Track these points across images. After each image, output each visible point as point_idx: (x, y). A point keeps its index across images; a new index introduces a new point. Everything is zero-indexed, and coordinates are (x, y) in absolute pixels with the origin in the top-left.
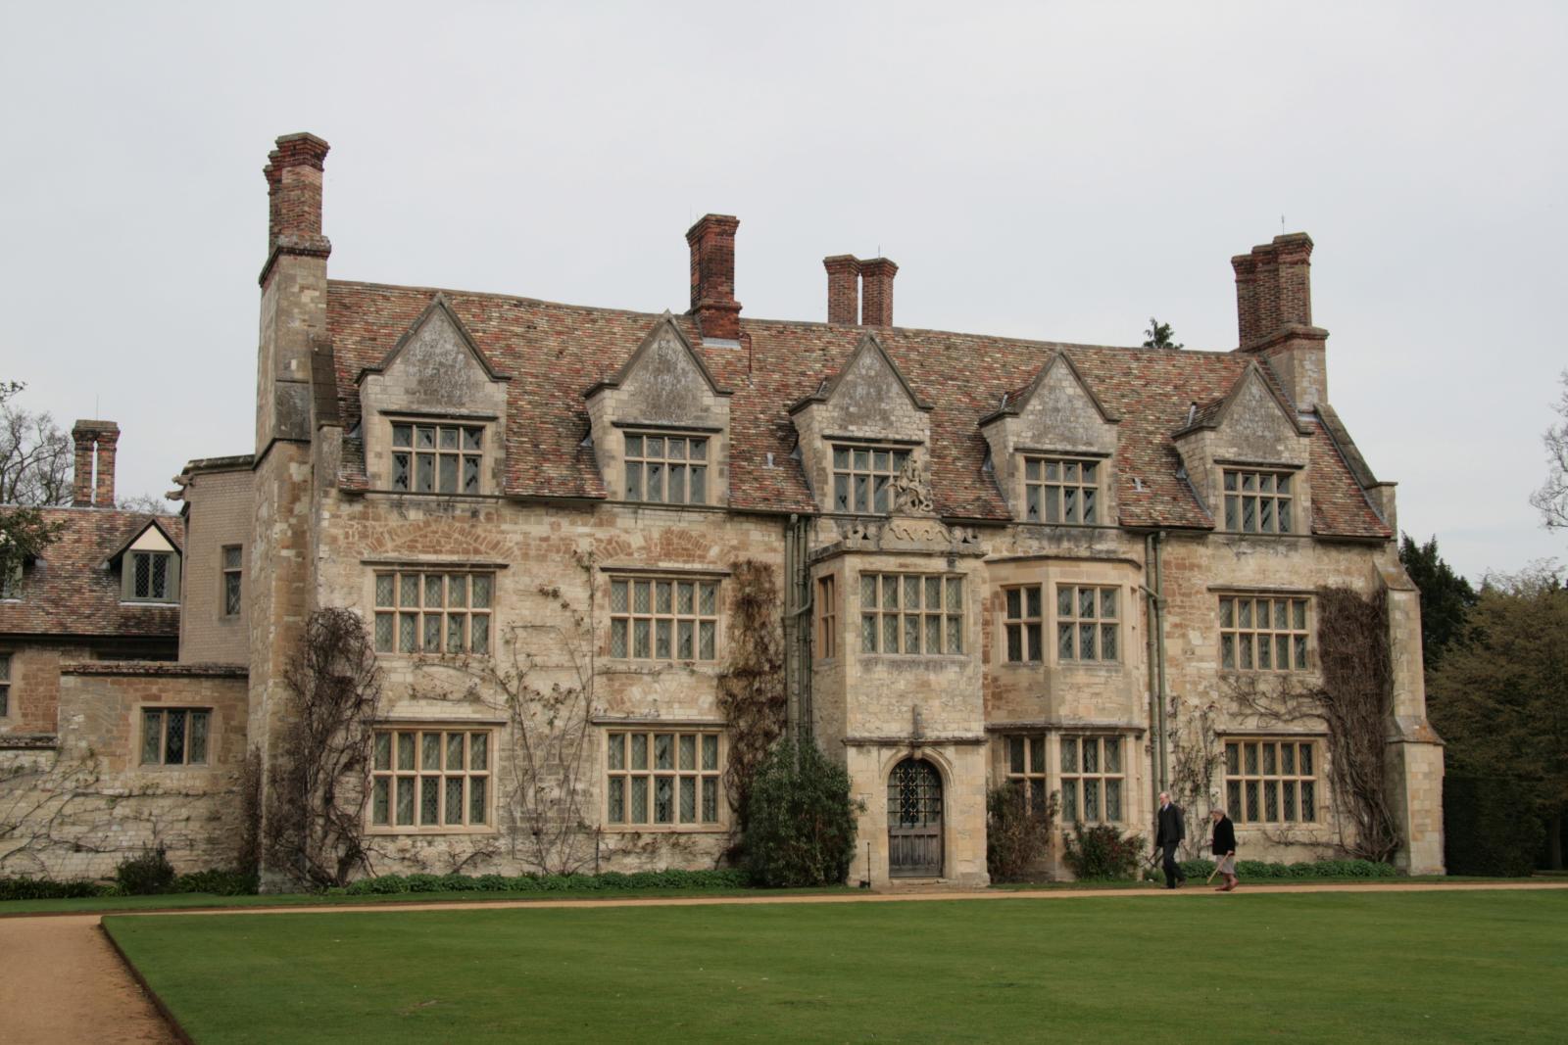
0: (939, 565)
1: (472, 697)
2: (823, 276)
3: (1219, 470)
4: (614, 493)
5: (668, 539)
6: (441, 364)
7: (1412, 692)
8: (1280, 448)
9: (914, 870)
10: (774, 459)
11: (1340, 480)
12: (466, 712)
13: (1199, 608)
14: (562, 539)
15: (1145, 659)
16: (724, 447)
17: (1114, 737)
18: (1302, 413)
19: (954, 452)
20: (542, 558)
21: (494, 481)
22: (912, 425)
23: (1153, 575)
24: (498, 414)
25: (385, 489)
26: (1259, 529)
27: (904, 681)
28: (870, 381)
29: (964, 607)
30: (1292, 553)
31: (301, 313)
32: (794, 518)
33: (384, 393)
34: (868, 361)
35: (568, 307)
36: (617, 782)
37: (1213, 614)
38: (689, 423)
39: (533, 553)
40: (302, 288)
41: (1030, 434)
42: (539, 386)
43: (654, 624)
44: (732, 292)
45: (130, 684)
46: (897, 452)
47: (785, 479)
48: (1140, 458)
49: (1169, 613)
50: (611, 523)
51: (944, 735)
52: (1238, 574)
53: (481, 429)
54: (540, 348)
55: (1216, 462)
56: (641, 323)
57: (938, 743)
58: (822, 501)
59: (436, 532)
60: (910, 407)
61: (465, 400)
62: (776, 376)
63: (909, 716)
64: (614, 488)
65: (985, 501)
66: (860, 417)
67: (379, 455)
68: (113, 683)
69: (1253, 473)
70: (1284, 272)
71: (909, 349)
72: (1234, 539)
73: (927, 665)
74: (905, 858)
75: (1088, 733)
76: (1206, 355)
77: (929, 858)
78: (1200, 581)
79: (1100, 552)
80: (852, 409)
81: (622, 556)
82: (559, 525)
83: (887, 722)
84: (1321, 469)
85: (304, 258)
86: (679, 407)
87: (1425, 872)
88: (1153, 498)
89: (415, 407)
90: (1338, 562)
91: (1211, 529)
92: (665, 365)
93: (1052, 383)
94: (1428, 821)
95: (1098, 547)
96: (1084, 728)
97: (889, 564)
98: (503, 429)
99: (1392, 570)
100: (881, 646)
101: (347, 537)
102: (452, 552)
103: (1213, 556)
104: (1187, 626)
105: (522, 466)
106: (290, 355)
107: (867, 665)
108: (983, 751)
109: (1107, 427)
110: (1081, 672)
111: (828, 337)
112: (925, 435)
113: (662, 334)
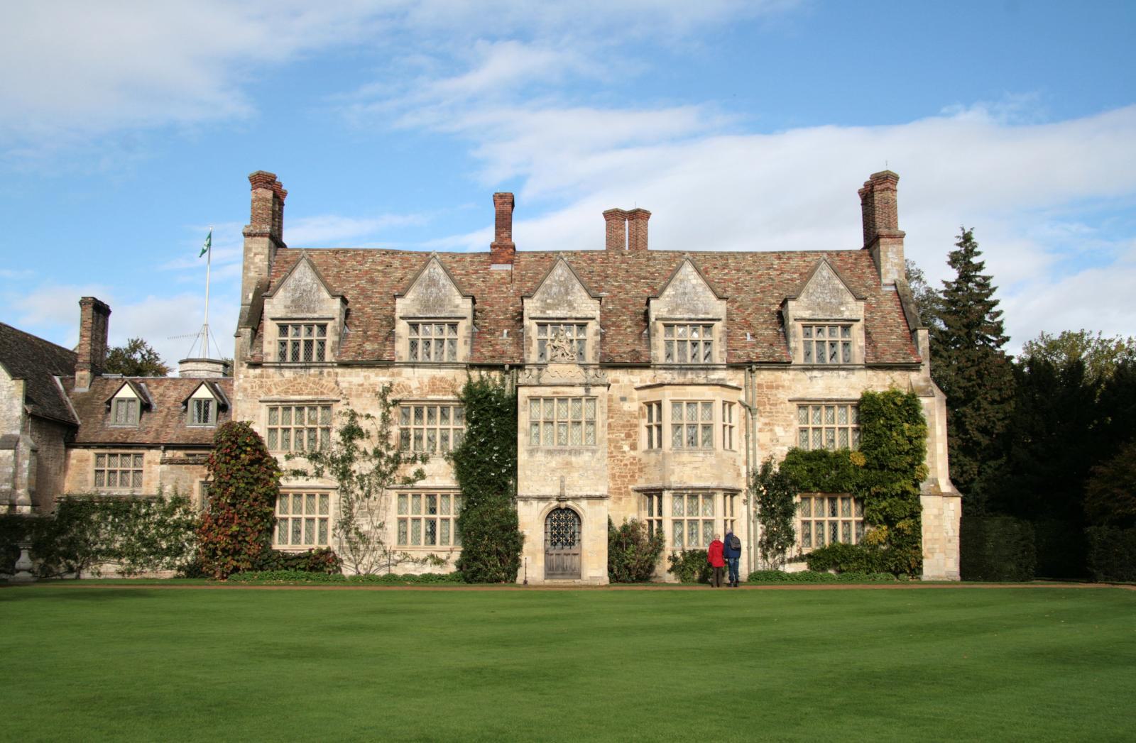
0: (580, 391)
1: (319, 474)
2: (603, 221)
3: (798, 325)
4: (401, 357)
5: (433, 382)
6: (304, 290)
7: (932, 463)
8: (843, 309)
9: (562, 574)
10: (508, 333)
12: (314, 482)
13: (783, 413)
14: (370, 385)
15: (744, 445)
16: (467, 328)
17: (709, 494)
18: (886, 285)
19: (629, 323)
20: (359, 396)
21: (332, 354)
22: (588, 308)
23: (750, 393)
24: (335, 316)
25: (272, 361)
26: (828, 361)
27: (555, 462)
28: (560, 284)
29: (597, 416)
30: (851, 376)
31: (255, 268)
32: (507, 367)
33: (275, 307)
34: (560, 272)
35: (416, 253)
36: (402, 521)
37: (792, 416)
38: (447, 315)
39: (354, 393)
40: (255, 254)
41: (666, 309)
42: (381, 299)
43: (425, 431)
44: (510, 237)
45: (193, 469)
48: (758, 319)
49: (761, 416)
50: (399, 374)
51: (580, 494)
52: (810, 390)
54: (389, 278)
55: (795, 320)
56: (457, 258)
57: (575, 499)
58: (529, 356)
59: (299, 383)
60: (587, 298)
61: (317, 309)
62: (529, 284)
63: (558, 482)
64: (400, 354)
65: (638, 352)
66: (555, 305)
68: (185, 468)
69: (824, 326)
70: (877, 196)
71: (623, 262)
72: (807, 368)
73: (570, 452)
74: (558, 567)
75: (690, 492)
76: (829, 253)
77: (573, 567)
78: (783, 395)
79: (713, 380)
80: (548, 301)
82: (369, 377)
83: (543, 486)
84: (887, 321)
85: (256, 238)
86: (440, 306)
87: (932, 579)
88: (754, 346)
89: (289, 315)
90: (884, 380)
91: (790, 363)
92: (433, 282)
93: (681, 278)
94: (937, 546)
96: (685, 489)
97: (547, 392)
98: (337, 325)
99: (922, 384)
100: (542, 443)
101: (252, 388)
102: (308, 394)
103: (793, 380)
104: (773, 424)
105: (353, 344)
106: (248, 291)
107: (532, 452)
108: (606, 502)
109: (719, 302)
110: (686, 454)
111: (572, 258)
112: (597, 314)
113: (430, 265)
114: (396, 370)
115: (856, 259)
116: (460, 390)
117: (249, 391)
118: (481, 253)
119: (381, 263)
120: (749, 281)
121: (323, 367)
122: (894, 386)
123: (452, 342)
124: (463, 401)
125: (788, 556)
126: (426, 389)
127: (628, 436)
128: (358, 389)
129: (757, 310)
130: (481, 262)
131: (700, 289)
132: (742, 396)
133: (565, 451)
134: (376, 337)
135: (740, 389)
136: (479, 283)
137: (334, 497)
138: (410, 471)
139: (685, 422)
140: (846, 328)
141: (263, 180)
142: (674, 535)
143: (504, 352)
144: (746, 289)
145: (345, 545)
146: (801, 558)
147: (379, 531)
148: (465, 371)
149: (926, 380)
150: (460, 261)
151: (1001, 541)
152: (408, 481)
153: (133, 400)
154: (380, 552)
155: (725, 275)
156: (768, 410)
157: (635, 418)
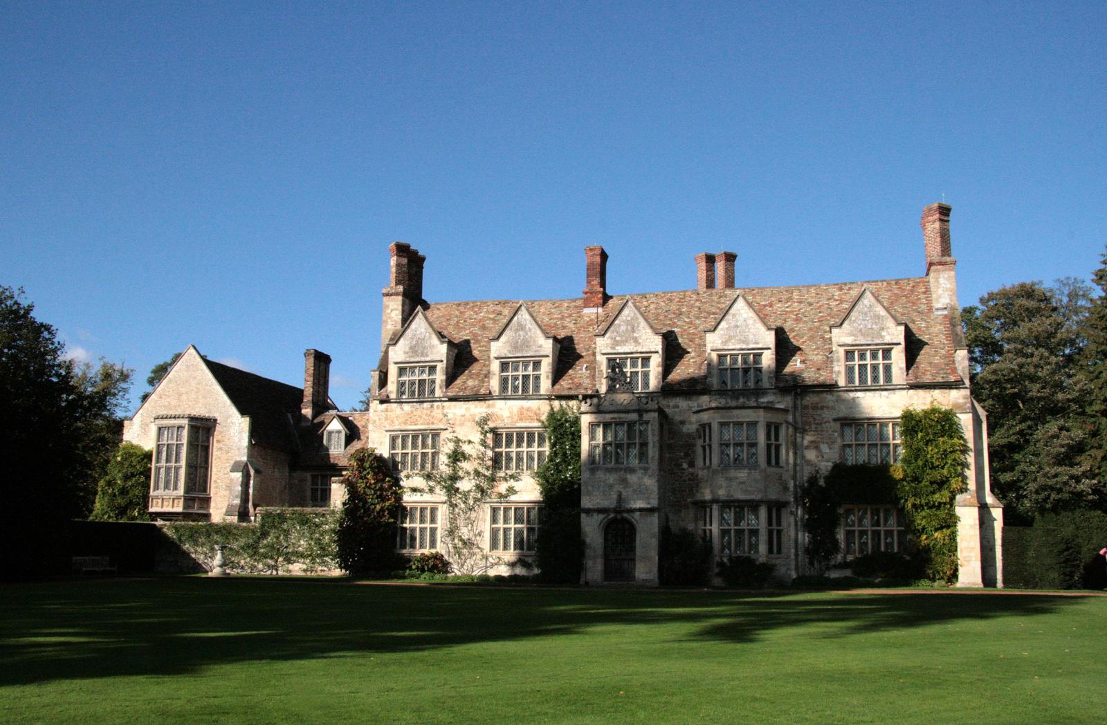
0: (634, 416)
1: (431, 490)
8: (884, 333)
11: (943, 349)
17: (754, 506)
18: (938, 309)
20: (462, 424)
28: (628, 323)
37: (836, 434)
39: (458, 423)
40: (392, 310)
46: (643, 359)
47: (587, 377)
50: (493, 406)
53: (435, 367)
55: (840, 346)
58: (600, 387)
60: (650, 334)
63: (615, 496)
67: (393, 382)
69: (866, 350)
71: (697, 300)
79: (763, 403)
81: (499, 422)
86: (527, 346)
87: (968, 586)
89: (408, 360)
92: (521, 327)
94: (972, 554)
95: (762, 400)
99: (961, 401)
101: (380, 419)
102: (422, 424)
108: (656, 515)
109: (768, 332)
110: (733, 471)
111: (653, 300)
112: (659, 348)
114: (491, 402)
115: (913, 287)
116: (544, 418)
117: (378, 423)
118: (577, 299)
119: (493, 312)
120: (809, 311)
121: (433, 401)
122: (935, 403)
123: (537, 378)
124: (545, 427)
125: (833, 563)
126: (516, 418)
127: (687, 455)
128: (461, 422)
129: (812, 338)
130: (576, 307)
131: (750, 322)
132: (790, 418)
133: (621, 469)
134: (478, 374)
135: (785, 411)
136: (571, 325)
137: (443, 511)
138: (502, 487)
139: (732, 442)
140: (887, 353)
141: (402, 250)
142: (722, 543)
143: (580, 384)
144: (804, 319)
145: (452, 550)
146: (844, 565)
147: (478, 538)
148: (547, 402)
149: (965, 398)
150: (558, 307)
151: (1044, 550)
152: (501, 496)
153: (339, 432)
154: (479, 557)
155: (787, 307)
156: (813, 429)
157: (694, 439)
